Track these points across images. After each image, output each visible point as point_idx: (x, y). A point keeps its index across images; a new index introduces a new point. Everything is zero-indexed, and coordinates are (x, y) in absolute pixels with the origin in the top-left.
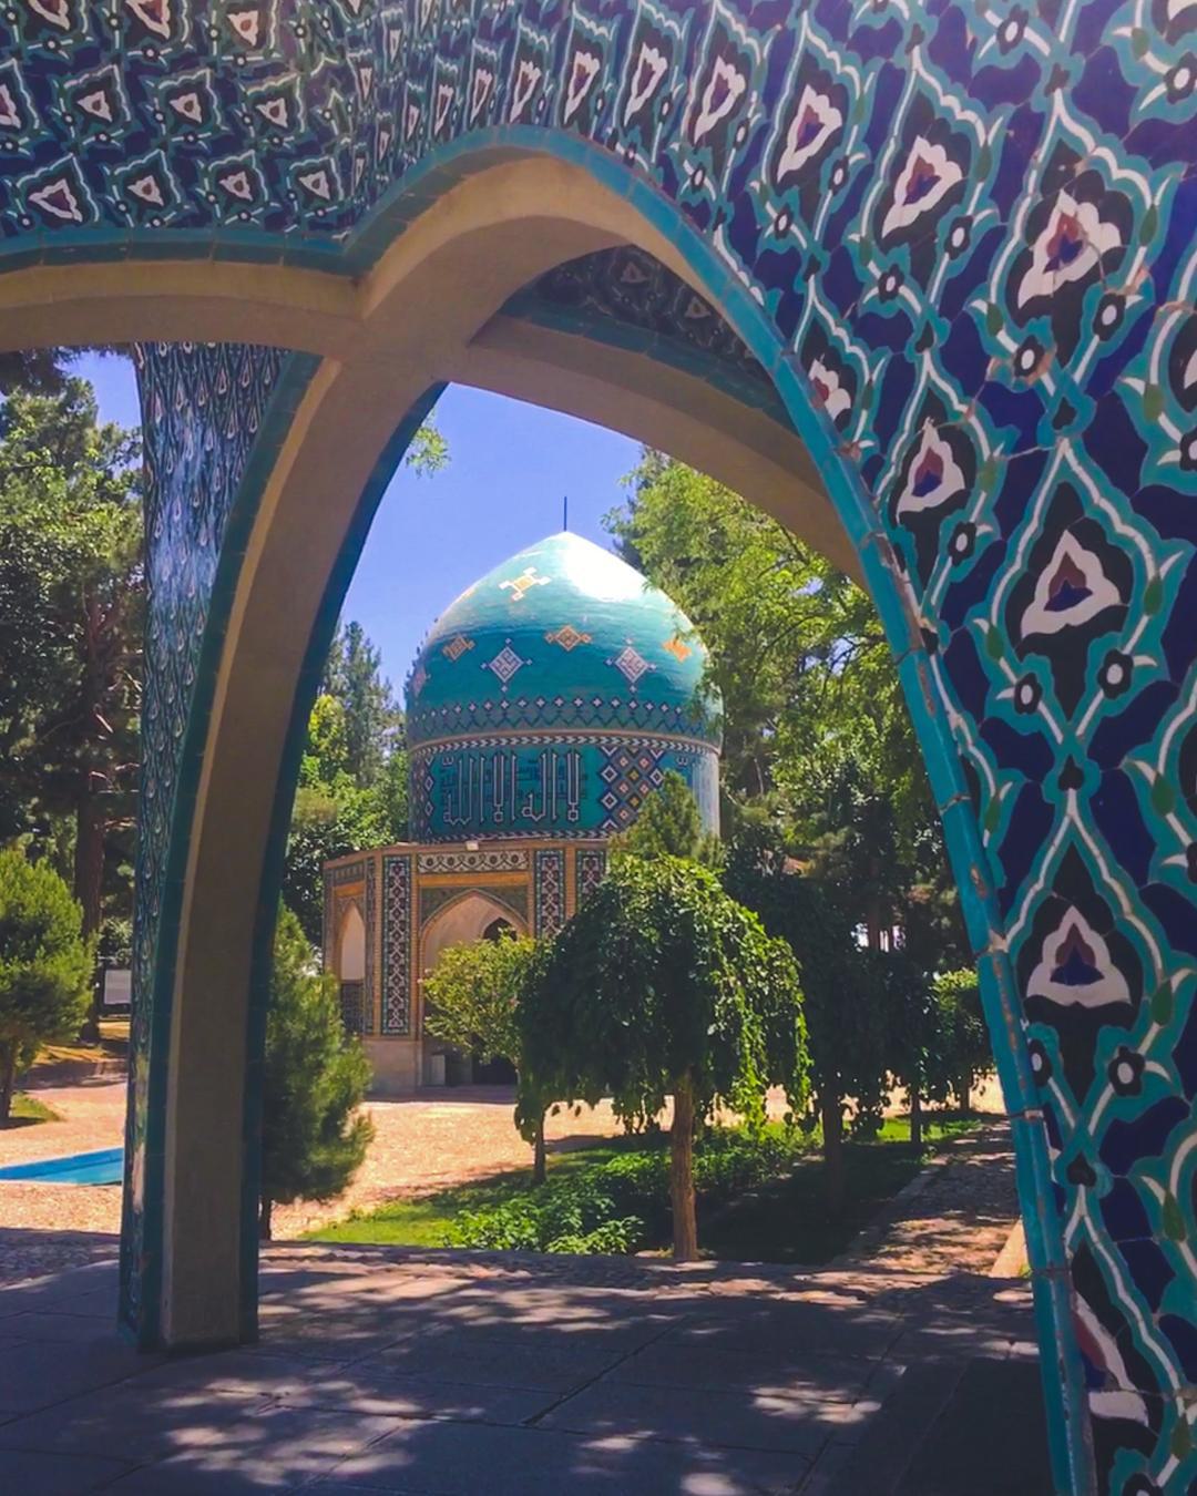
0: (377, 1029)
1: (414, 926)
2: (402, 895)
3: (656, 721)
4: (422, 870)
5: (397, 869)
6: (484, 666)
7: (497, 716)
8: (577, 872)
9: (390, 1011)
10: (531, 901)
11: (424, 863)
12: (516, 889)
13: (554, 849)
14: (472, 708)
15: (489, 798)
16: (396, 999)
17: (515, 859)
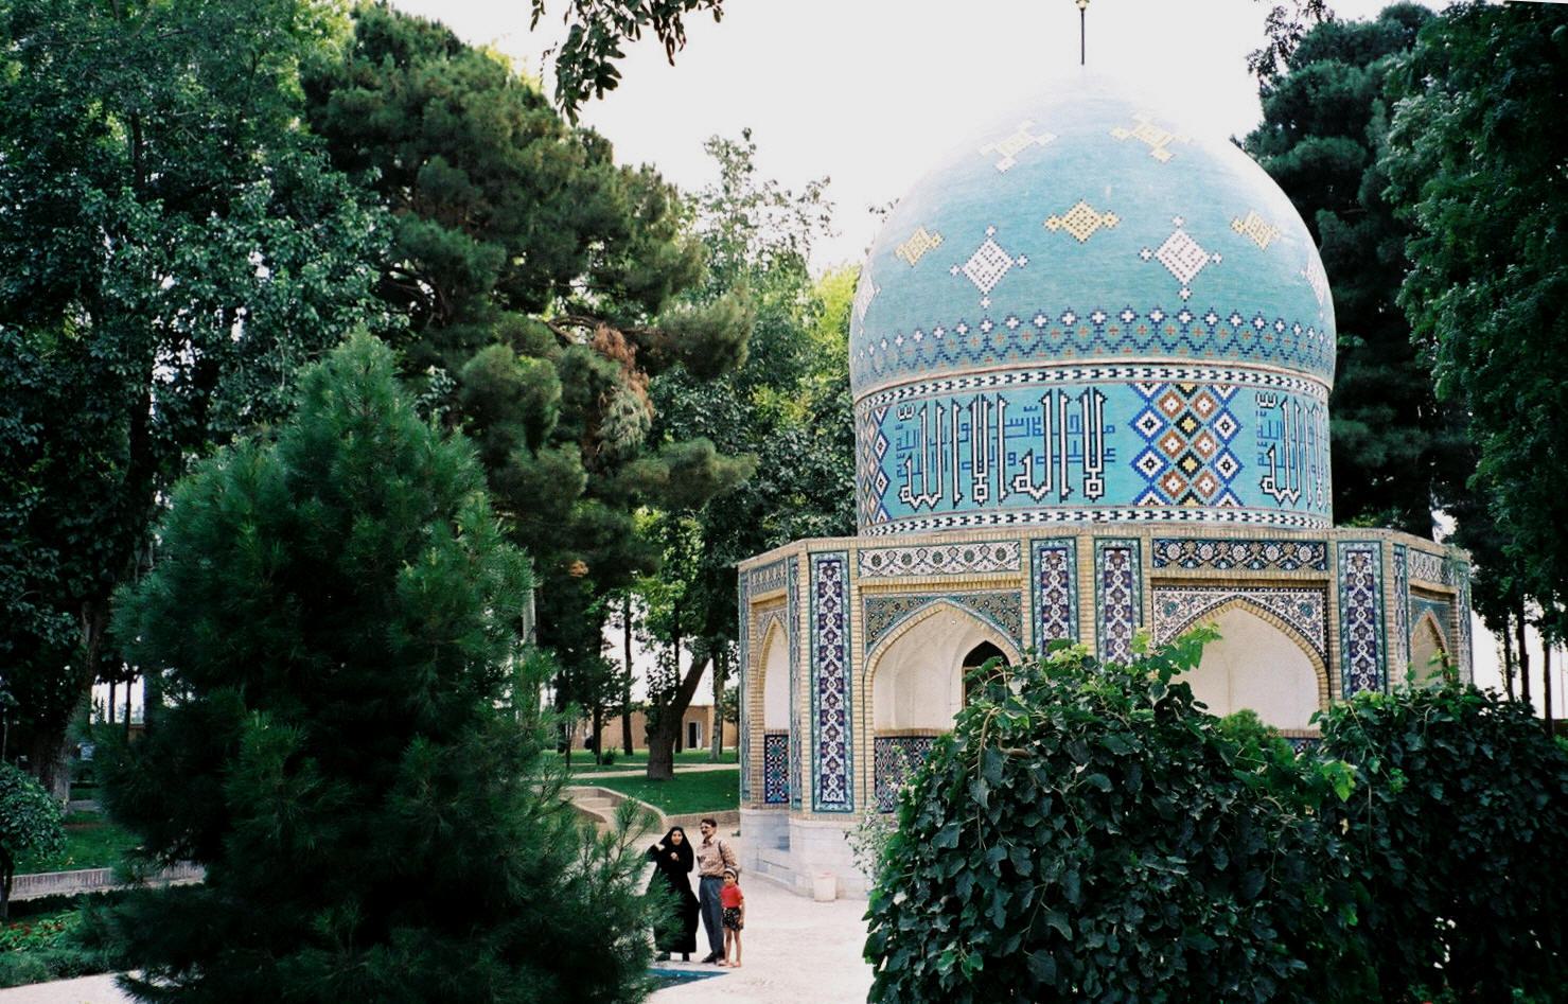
0: (807, 804)
1: (857, 649)
3: (1222, 341)
4: (866, 573)
6: (955, 271)
7: (975, 342)
8: (1096, 573)
9: (824, 777)
10: (1026, 618)
11: (868, 562)
12: (1003, 599)
13: (1059, 539)
14: (939, 333)
16: (833, 759)
17: (1001, 554)
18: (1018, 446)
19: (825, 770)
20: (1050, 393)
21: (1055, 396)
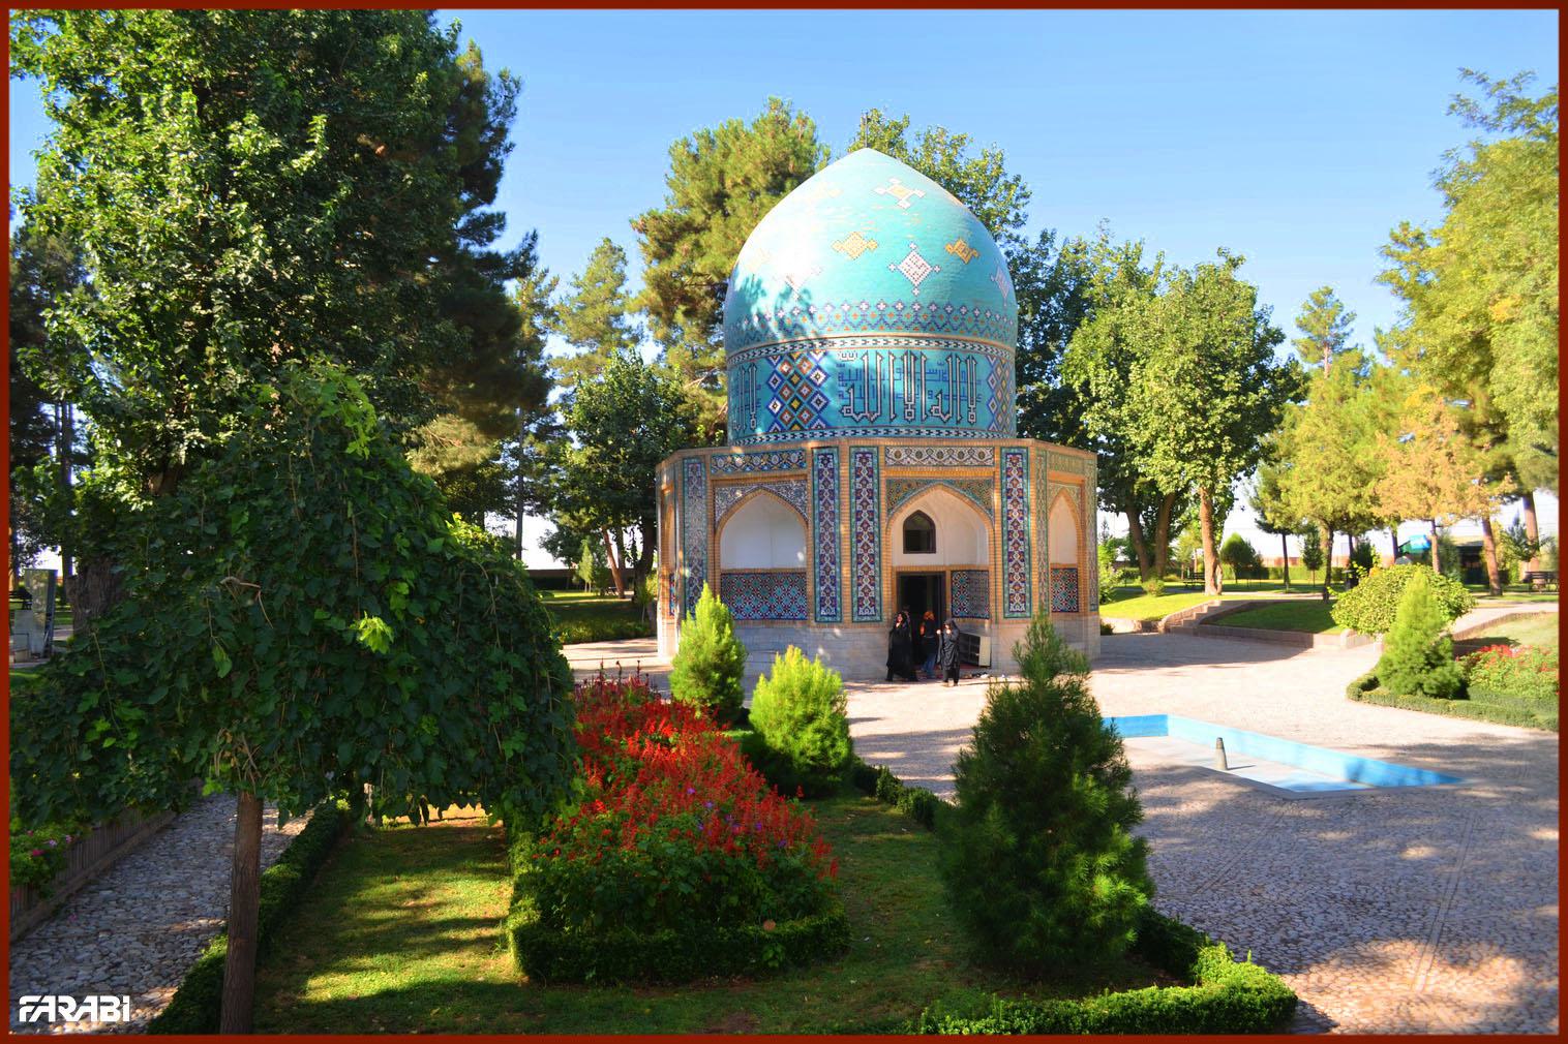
4: (890, 462)
5: (864, 458)
19: (861, 595)
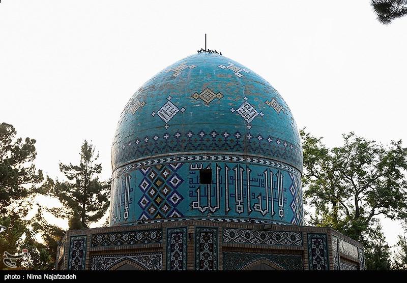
2: (211, 258)
15: (231, 195)
17: (293, 238)
18: (257, 191)
20: (267, 170)
21: (268, 170)
